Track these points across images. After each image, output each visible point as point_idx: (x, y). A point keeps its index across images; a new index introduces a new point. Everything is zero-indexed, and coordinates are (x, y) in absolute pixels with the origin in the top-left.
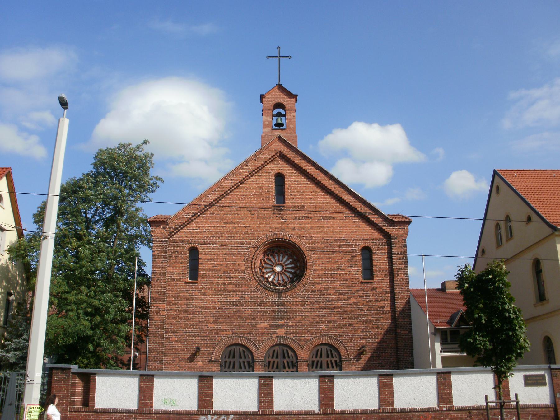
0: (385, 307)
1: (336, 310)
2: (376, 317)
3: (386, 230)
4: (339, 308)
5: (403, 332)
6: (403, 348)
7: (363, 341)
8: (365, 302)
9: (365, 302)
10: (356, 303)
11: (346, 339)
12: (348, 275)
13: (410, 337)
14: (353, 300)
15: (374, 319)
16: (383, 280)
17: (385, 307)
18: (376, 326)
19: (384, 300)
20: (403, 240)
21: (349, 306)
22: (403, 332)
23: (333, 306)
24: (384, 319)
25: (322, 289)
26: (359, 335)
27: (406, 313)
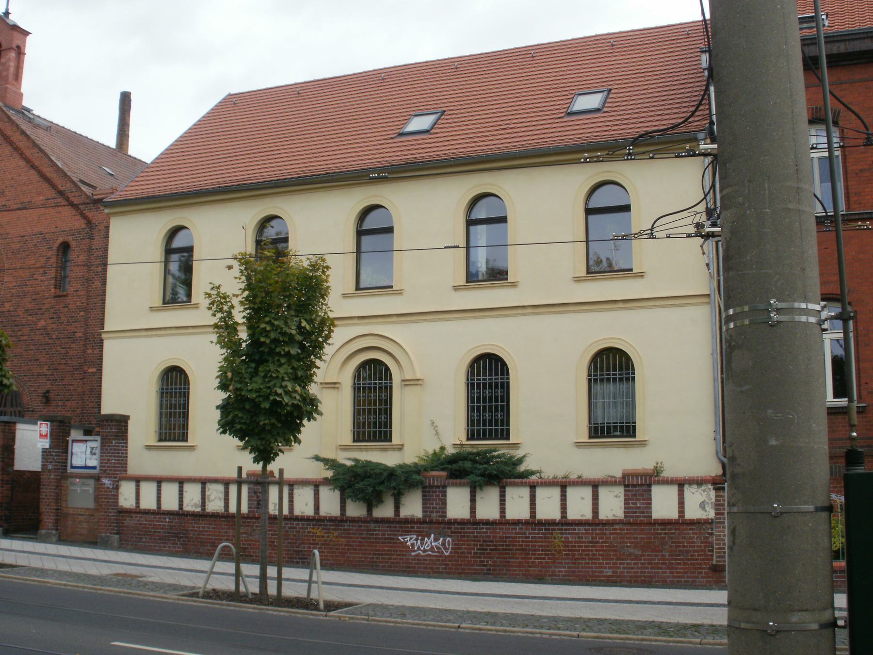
0: (76, 332)
1: (23, 338)
2: (65, 348)
3: (87, 214)
4: (27, 335)
5: (90, 370)
6: (88, 394)
7: (48, 383)
8: (54, 326)
9: (54, 326)
10: (45, 328)
11: (31, 381)
12: (41, 286)
13: (99, 378)
14: (42, 323)
15: (63, 351)
16: (78, 291)
17: (76, 332)
18: (63, 361)
19: (76, 322)
20: (105, 227)
21: (37, 332)
22: (90, 370)
23: (20, 333)
24: (73, 350)
25: (11, 309)
26: (44, 375)
27: (97, 341)
